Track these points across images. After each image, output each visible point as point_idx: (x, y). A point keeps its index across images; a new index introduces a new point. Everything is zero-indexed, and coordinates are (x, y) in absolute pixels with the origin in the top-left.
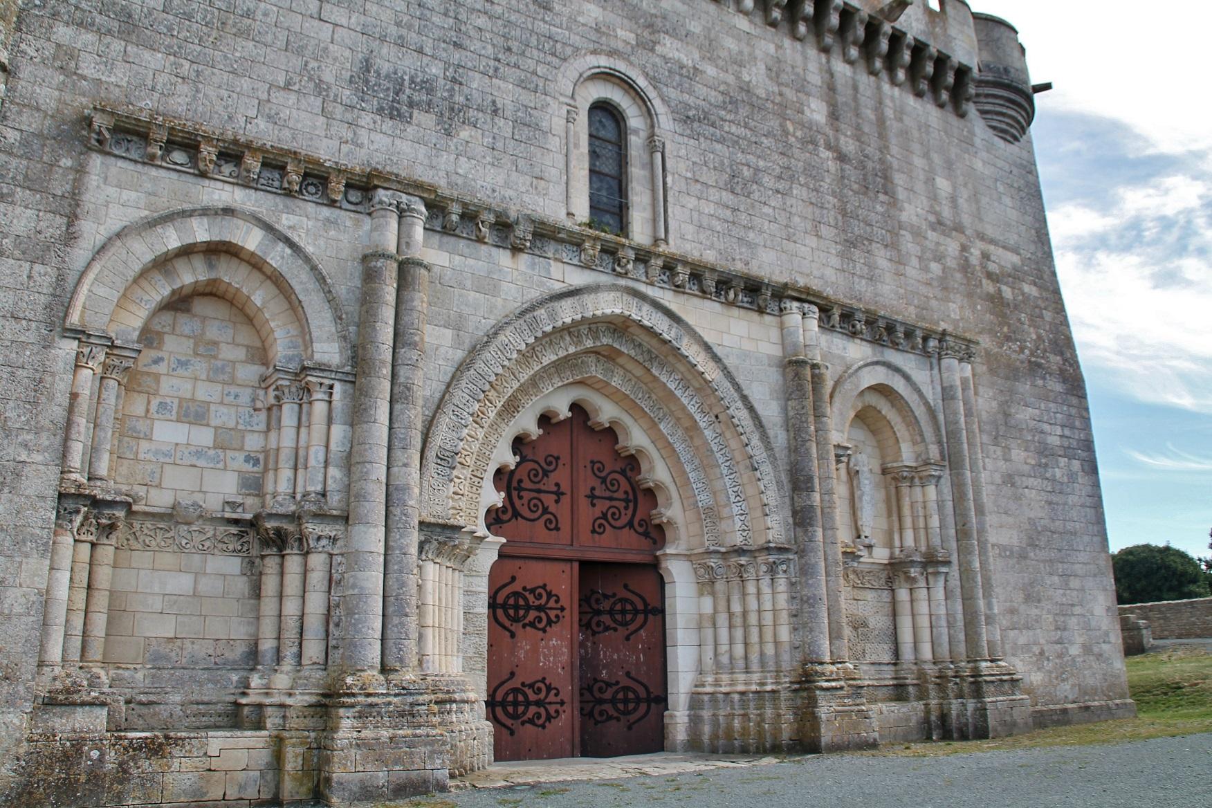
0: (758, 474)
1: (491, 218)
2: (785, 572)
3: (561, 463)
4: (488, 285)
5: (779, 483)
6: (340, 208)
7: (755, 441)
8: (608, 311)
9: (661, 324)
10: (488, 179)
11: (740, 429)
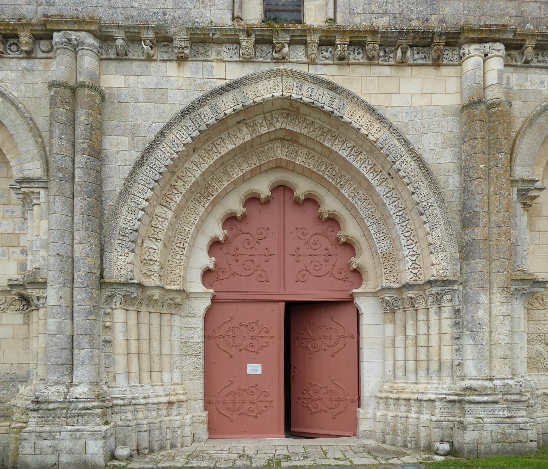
0: (424, 218)
1: (151, 35)
2: (451, 301)
4: (157, 95)
5: (449, 224)
6: (36, 58)
7: (424, 187)
8: (268, 96)
9: (324, 98)
10: (158, 6)
11: (406, 180)
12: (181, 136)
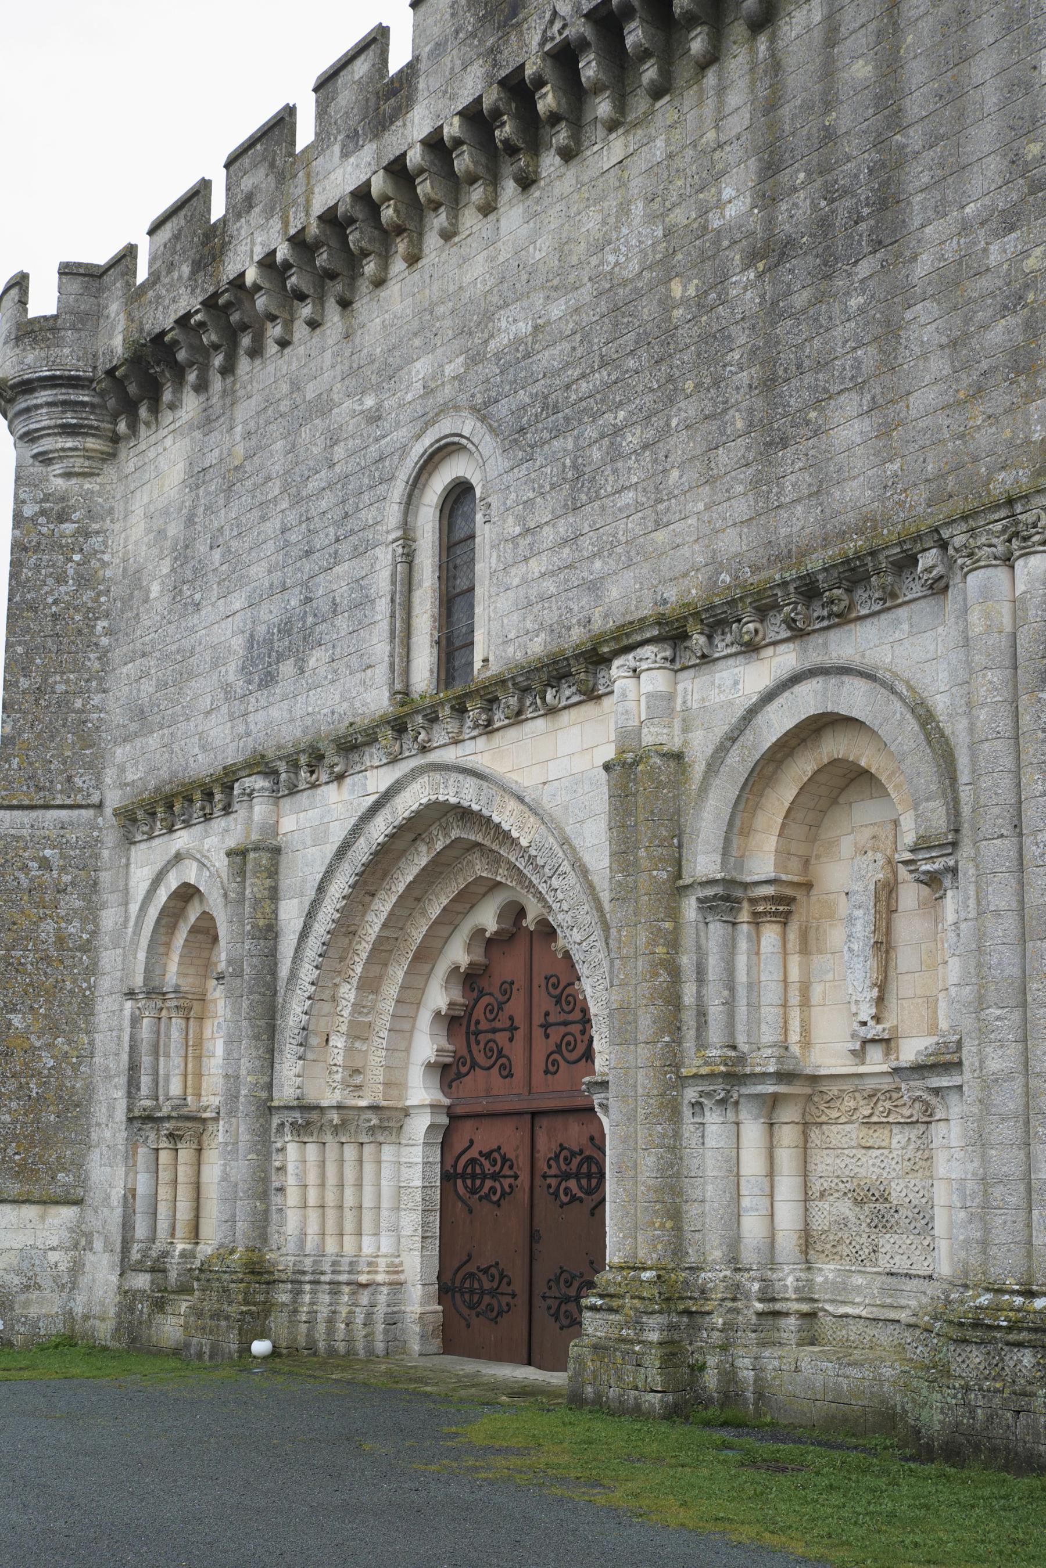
3: (515, 987)
12: (340, 886)
